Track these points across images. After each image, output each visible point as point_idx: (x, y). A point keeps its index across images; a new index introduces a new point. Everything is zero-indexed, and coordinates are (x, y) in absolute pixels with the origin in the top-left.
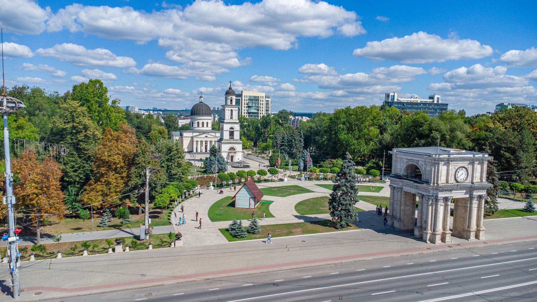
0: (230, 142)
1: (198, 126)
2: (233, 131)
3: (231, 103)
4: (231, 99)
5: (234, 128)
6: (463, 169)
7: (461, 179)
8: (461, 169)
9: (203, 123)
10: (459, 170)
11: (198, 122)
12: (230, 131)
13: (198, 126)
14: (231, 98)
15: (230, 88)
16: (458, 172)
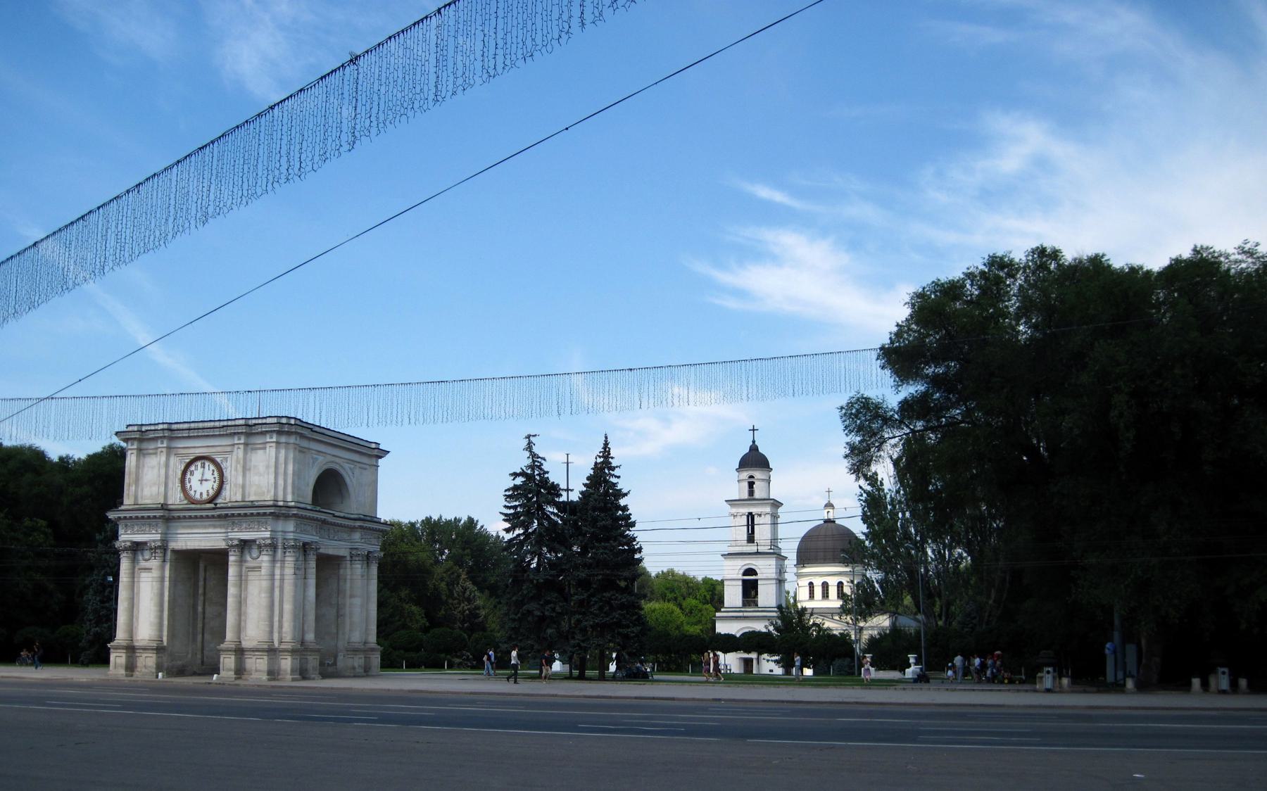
0: (741, 614)
1: (812, 595)
2: (756, 581)
3: (751, 493)
4: (751, 480)
5: (758, 571)
6: (207, 464)
7: (201, 494)
8: (199, 463)
9: (825, 586)
10: (193, 468)
11: (811, 585)
12: (744, 581)
13: (812, 595)
14: (751, 477)
15: (754, 448)
16: (192, 473)
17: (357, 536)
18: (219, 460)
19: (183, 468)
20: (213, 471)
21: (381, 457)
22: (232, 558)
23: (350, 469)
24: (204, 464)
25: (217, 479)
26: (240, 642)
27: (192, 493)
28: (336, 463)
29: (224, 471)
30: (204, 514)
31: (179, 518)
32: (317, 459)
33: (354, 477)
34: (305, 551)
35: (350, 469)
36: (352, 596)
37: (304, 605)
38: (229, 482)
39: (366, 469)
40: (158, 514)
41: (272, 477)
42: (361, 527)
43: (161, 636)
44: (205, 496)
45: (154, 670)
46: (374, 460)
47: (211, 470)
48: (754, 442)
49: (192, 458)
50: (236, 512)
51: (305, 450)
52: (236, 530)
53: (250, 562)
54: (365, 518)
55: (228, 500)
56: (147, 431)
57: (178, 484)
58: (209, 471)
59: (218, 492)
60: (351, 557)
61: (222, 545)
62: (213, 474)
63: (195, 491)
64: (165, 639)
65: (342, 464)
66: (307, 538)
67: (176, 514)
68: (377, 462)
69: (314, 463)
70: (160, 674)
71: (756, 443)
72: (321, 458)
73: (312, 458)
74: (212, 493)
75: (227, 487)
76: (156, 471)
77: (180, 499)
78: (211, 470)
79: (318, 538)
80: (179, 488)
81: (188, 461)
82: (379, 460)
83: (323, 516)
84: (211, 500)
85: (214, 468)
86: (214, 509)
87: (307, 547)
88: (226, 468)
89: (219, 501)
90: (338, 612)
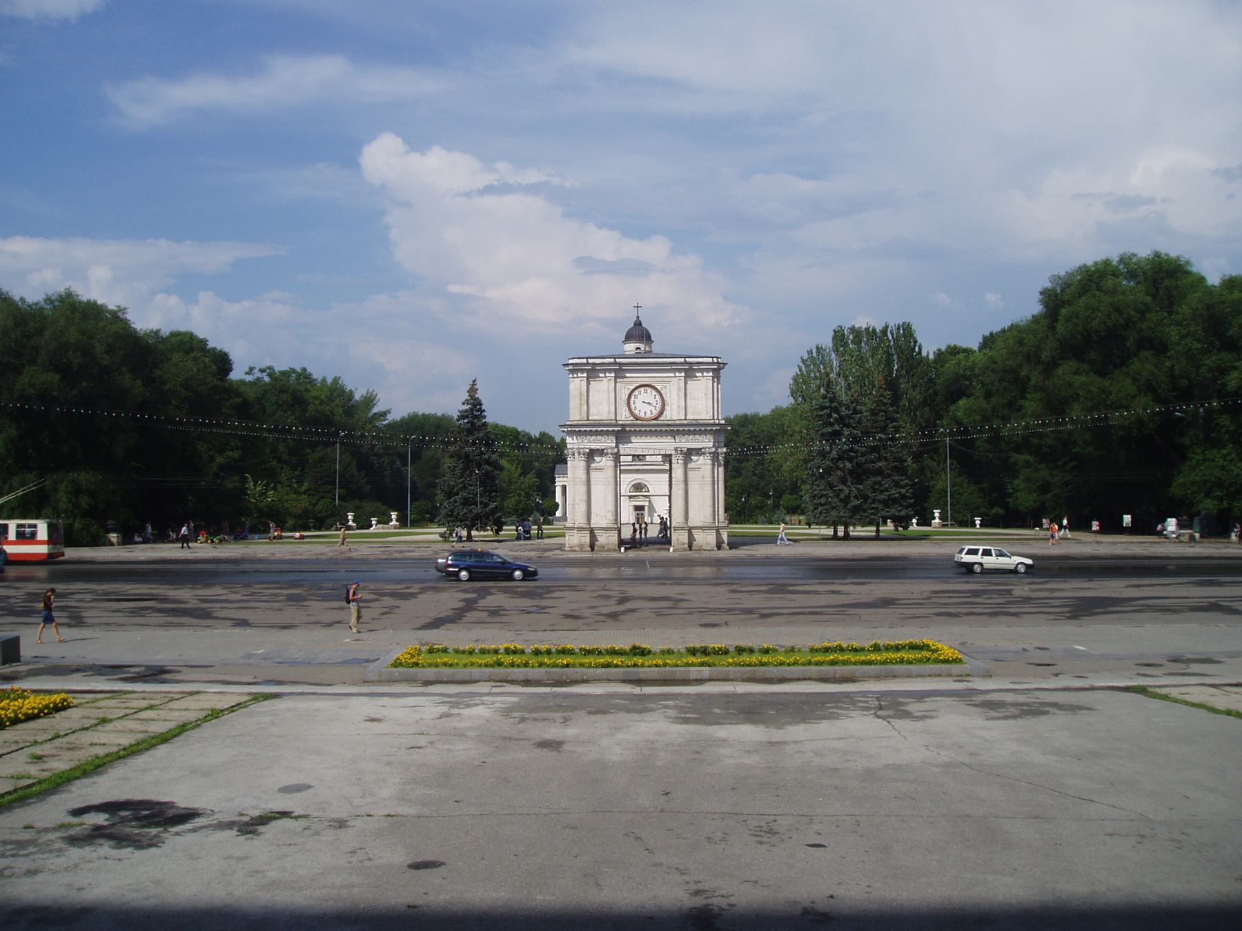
6: (649, 390)
7: (645, 413)
8: (642, 389)
10: (636, 392)
15: (638, 324)
16: (636, 397)
18: (658, 387)
20: (655, 395)
44: (649, 415)
47: (653, 394)
48: (638, 317)
49: (637, 385)
52: (683, 441)
58: (650, 396)
59: (661, 413)
63: (640, 411)
71: (640, 318)
78: (653, 394)
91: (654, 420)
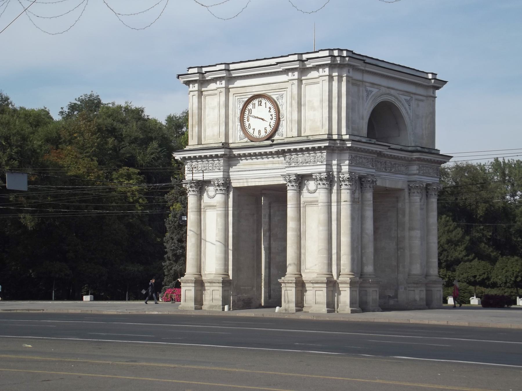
6: (264, 101)
7: (259, 131)
8: (256, 102)
10: (250, 106)
16: (250, 111)
17: (414, 169)
18: (274, 97)
19: (241, 107)
20: (270, 108)
21: (438, 88)
22: (291, 194)
23: (405, 100)
24: (261, 101)
25: (274, 116)
26: (301, 275)
27: (251, 131)
28: (391, 95)
29: (280, 107)
30: (262, 151)
31: (239, 156)
32: (372, 92)
33: (410, 109)
34: (362, 184)
35: (405, 100)
36: (411, 229)
37: (362, 237)
38: (285, 118)
39: (422, 101)
40: (220, 152)
41: (326, 110)
42: (419, 159)
43: (227, 270)
44: (263, 134)
45: (220, 303)
46: (431, 90)
47: (268, 107)
49: (250, 96)
50: (292, 147)
51: (359, 83)
52: (293, 165)
53: (306, 195)
54: (423, 150)
55: (284, 136)
56: (206, 72)
57: (238, 123)
59: (276, 129)
60: (410, 190)
61: (282, 181)
62: (269, 112)
63: (254, 129)
64: (230, 273)
65: (397, 96)
66: (363, 171)
67: (236, 152)
68: (434, 93)
69: (368, 96)
70: (226, 307)
72: (375, 91)
73: (367, 91)
74: (269, 130)
75: (283, 123)
76: (216, 111)
77: (240, 138)
79: (374, 171)
80: (239, 127)
81: (246, 99)
82: (437, 91)
83: (378, 149)
84: (270, 137)
85: (271, 106)
86: (271, 145)
87: (363, 180)
88: (282, 105)
89: (276, 137)
90: (397, 245)
91: (267, 139)
